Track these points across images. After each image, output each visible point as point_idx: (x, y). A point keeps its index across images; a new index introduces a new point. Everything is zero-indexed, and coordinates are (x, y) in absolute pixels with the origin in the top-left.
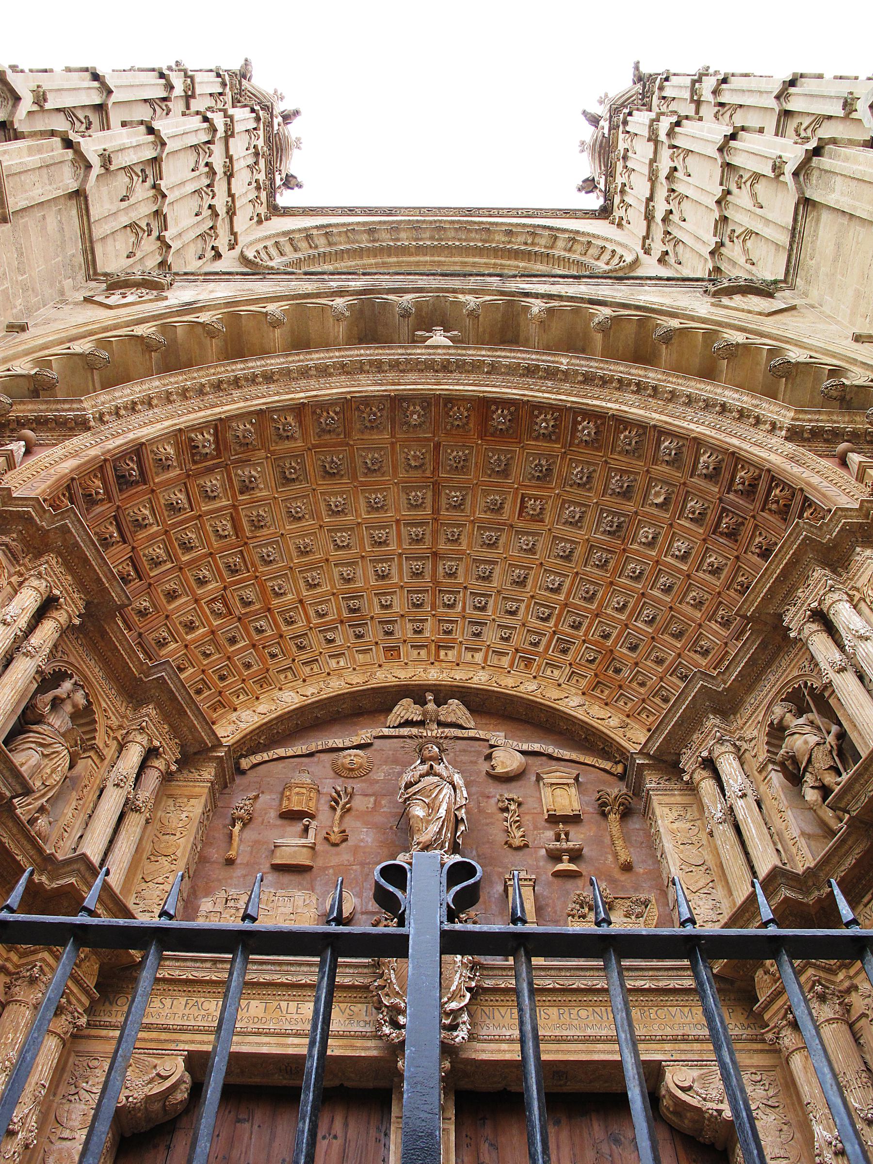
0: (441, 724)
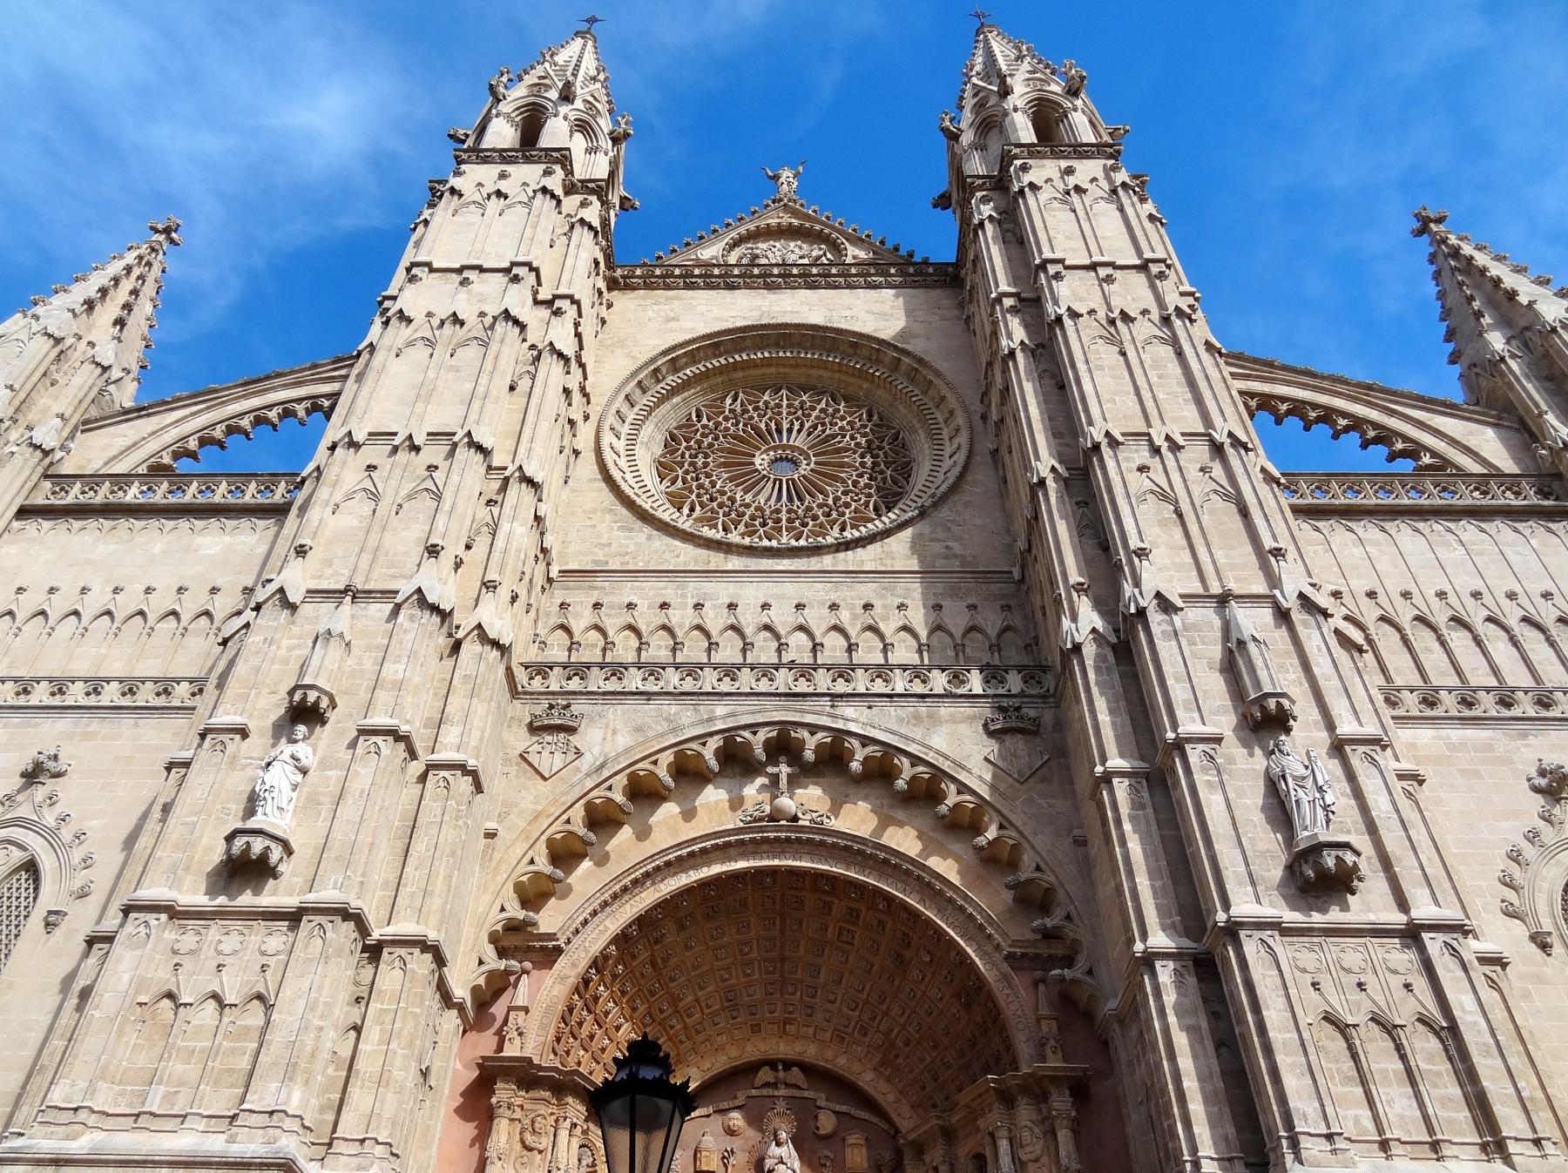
0: (788, 1085)
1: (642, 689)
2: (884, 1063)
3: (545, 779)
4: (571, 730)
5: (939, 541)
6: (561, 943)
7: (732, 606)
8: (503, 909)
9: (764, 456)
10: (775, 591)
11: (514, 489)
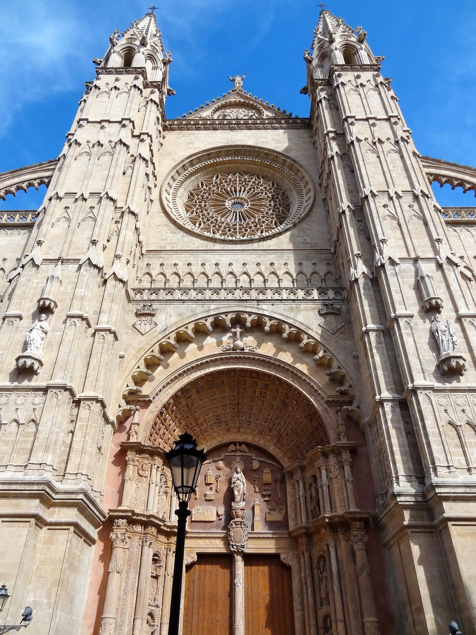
0: (240, 451)
1: (181, 298)
2: (278, 442)
3: (143, 335)
4: (153, 315)
5: (301, 237)
6: (151, 398)
7: (217, 264)
8: (128, 386)
9: (229, 202)
10: (234, 258)
11: (126, 216)
